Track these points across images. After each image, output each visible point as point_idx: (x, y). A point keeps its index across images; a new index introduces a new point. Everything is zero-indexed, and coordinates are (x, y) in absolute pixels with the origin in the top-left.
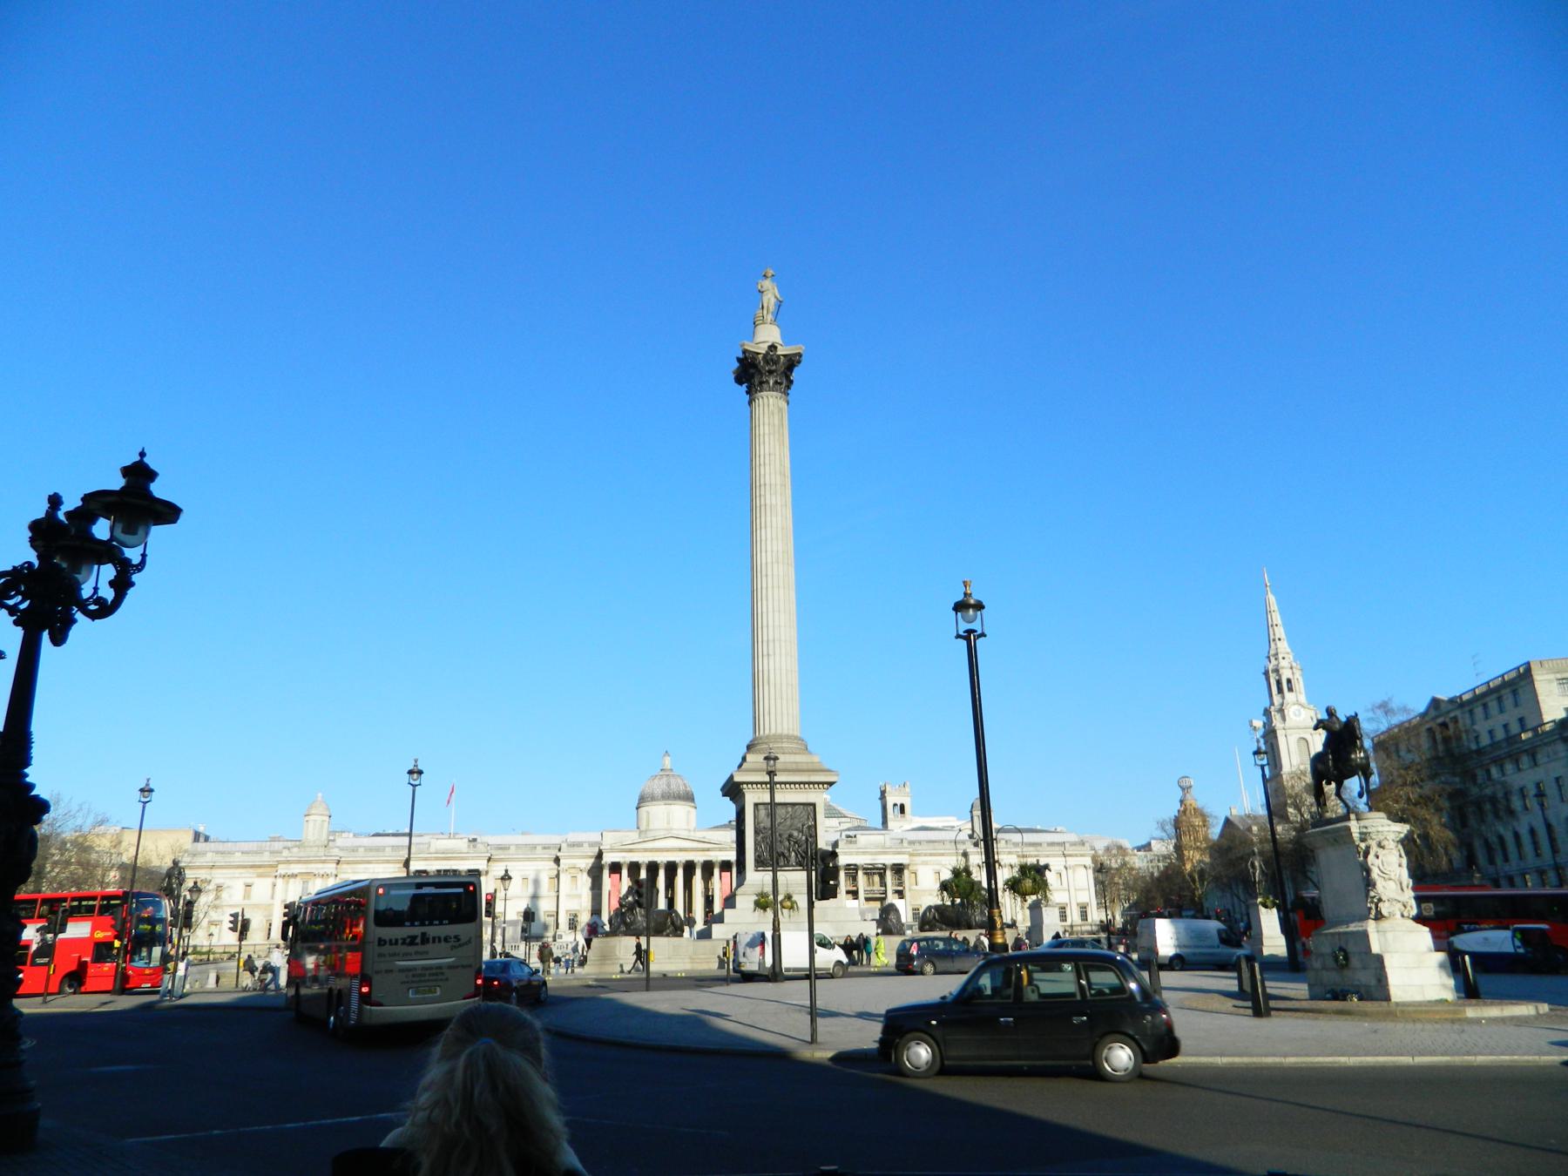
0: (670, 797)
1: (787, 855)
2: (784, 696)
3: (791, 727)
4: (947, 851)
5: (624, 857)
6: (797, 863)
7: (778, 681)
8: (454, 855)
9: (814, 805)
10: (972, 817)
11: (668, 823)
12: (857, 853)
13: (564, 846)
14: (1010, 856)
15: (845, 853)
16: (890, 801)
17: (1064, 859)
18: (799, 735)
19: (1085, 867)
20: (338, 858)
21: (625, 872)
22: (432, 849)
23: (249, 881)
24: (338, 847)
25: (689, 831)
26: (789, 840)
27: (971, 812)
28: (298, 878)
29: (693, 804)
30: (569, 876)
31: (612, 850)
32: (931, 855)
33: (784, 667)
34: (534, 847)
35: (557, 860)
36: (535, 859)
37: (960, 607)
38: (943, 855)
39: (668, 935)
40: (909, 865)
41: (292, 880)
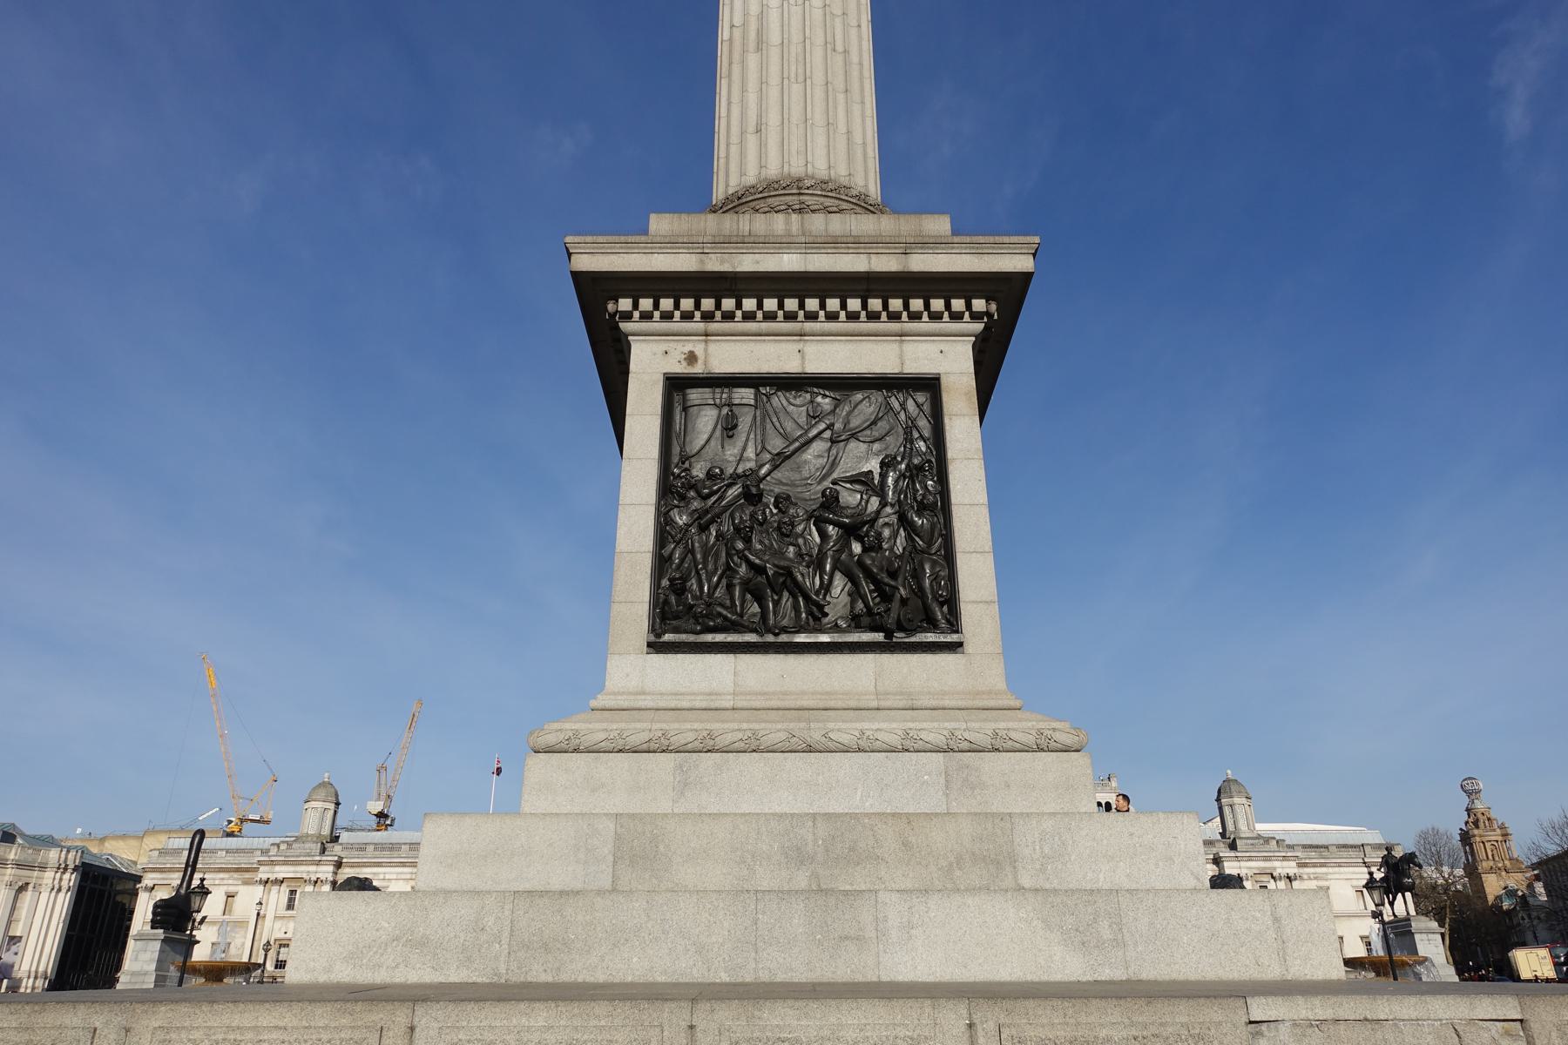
9: (930, 385)
10: (1221, 809)
14: (1285, 864)
17: (1365, 870)
20: (336, 858)
23: (232, 889)
26: (820, 523)
27: (1218, 800)
28: (284, 885)
41: (275, 889)
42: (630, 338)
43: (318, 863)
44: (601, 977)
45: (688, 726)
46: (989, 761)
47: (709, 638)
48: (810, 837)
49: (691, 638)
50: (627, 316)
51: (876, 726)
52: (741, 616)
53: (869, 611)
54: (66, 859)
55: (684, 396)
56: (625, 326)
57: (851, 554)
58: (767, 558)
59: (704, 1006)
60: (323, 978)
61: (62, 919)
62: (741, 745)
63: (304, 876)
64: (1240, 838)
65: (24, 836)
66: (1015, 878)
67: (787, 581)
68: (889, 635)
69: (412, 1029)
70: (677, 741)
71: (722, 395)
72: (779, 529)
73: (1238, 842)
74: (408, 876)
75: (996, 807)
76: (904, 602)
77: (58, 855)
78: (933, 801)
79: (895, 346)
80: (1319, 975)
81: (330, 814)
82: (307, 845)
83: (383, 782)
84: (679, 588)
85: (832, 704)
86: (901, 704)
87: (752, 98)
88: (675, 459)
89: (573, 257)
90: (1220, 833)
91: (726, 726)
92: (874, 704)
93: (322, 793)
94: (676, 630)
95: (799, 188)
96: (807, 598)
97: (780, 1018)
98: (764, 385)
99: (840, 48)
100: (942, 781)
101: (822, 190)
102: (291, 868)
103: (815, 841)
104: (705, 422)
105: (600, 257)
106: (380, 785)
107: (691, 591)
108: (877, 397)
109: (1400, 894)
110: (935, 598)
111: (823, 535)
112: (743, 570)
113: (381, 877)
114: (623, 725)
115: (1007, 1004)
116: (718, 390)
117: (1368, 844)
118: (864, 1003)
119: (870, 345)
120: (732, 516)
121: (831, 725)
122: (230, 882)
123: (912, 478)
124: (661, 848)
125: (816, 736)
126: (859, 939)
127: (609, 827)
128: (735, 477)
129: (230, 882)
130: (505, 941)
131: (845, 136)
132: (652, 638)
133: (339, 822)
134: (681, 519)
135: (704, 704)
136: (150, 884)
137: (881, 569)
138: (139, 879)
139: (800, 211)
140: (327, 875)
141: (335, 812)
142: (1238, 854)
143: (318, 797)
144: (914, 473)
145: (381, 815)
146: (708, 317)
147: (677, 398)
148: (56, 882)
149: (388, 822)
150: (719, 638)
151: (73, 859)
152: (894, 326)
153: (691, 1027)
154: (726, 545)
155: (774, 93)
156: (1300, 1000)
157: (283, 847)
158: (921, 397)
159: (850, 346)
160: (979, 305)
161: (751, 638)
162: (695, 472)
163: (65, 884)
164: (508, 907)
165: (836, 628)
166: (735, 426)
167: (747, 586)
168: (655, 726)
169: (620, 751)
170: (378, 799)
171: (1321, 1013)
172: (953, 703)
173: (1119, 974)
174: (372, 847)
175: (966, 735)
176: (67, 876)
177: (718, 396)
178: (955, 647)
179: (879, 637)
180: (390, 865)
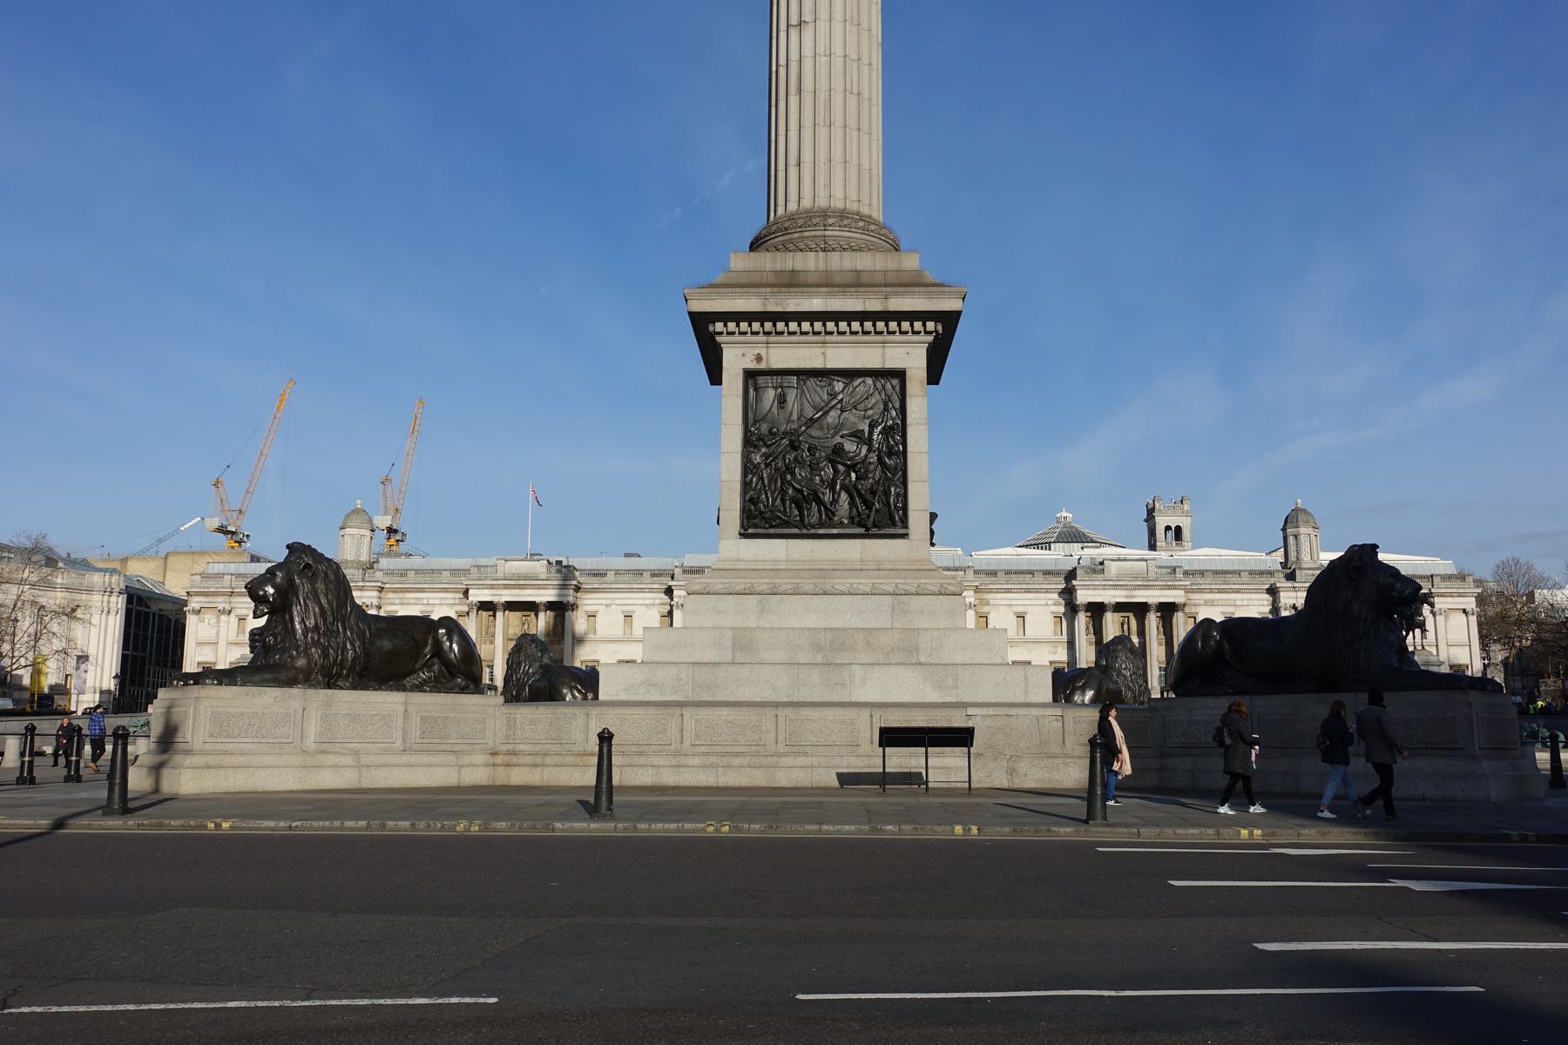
2: (838, 121)
4: (1245, 587)
6: (851, 518)
7: (823, 85)
8: (527, 582)
9: (900, 375)
10: (1285, 539)
12: (1105, 587)
13: (678, 572)
15: (1087, 587)
16: (1161, 522)
18: (877, 214)
19: (1464, 611)
20: (379, 584)
22: (500, 574)
24: (382, 570)
26: (833, 463)
27: (1284, 530)
32: (1220, 591)
33: (838, 51)
34: (639, 573)
35: (669, 592)
36: (641, 590)
38: (1237, 591)
39: (419, 688)
40: (1184, 605)
42: (722, 345)
44: (732, 699)
45: (764, 581)
46: (915, 602)
47: (772, 531)
48: (823, 639)
49: (763, 531)
50: (721, 333)
51: (858, 581)
53: (859, 514)
54: (110, 582)
55: (755, 381)
56: (718, 339)
57: (851, 481)
58: (803, 484)
59: (780, 708)
60: (615, 699)
61: (116, 639)
62: (791, 591)
64: (1301, 569)
66: (918, 658)
68: (867, 530)
69: (682, 715)
70: (759, 589)
71: (777, 380)
72: (810, 466)
73: (1297, 571)
74: (452, 602)
75: (916, 625)
76: (877, 511)
77: (102, 580)
78: (884, 621)
79: (881, 349)
80: (1041, 701)
85: (838, 567)
86: (873, 567)
88: (751, 422)
89: (689, 302)
90: (1281, 563)
91: (782, 581)
92: (859, 567)
93: (357, 520)
94: (756, 526)
95: (825, 226)
96: (826, 507)
97: (806, 712)
98: (802, 375)
99: (855, 91)
100: (890, 609)
101: (840, 226)
103: (826, 640)
104: (770, 395)
105: (705, 302)
107: (762, 502)
108: (869, 381)
109: (1411, 633)
110: (895, 506)
111: (836, 471)
112: (790, 491)
113: (425, 602)
114: (730, 580)
115: (885, 709)
116: (775, 377)
117: (1438, 575)
118: (835, 708)
119: (864, 349)
120: (784, 457)
121: (836, 581)
123: (887, 435)
124: (754, 643)
125: (828, 587)
127: (729, 634)
128: (785, 433)
130: (690, 685)
131: (856, 168)
132: (742, 531)
134: (757, 458)
135: (771, 567)
136: (197, 607)
137: (866, 491)
138: (185, 603)
139: (824, 250)
140: (371, 600)
142: (1295, 585)
143: (354, 524)
144: (887, 431)
145: (391, 531)
148: (105, 604)
150: (779, 531)
151: (117, 582)
152: (879, 338)
153: (776, 715)
154: (781, 476)
156: (985, 708)
158: (895, 382)
159: (852, 350)
160: (930, 325)
161: (796, 531)
162: (763, 430)
163: (113, 605)
164: (690, 670)
165: (841, 525)
166: (785, 401)
167: (793, 500)
168: (747, 581)
169: (730, 594)
170: (386, 513)
171: (992, 713)
172: (901, 567)
173: (954, 700)
174: (413, 573)
175: (904, 587)
176: (113, 599)
177: (775, 381)
178: (904, 536)
179: (862, 531)
180: (433, 590)
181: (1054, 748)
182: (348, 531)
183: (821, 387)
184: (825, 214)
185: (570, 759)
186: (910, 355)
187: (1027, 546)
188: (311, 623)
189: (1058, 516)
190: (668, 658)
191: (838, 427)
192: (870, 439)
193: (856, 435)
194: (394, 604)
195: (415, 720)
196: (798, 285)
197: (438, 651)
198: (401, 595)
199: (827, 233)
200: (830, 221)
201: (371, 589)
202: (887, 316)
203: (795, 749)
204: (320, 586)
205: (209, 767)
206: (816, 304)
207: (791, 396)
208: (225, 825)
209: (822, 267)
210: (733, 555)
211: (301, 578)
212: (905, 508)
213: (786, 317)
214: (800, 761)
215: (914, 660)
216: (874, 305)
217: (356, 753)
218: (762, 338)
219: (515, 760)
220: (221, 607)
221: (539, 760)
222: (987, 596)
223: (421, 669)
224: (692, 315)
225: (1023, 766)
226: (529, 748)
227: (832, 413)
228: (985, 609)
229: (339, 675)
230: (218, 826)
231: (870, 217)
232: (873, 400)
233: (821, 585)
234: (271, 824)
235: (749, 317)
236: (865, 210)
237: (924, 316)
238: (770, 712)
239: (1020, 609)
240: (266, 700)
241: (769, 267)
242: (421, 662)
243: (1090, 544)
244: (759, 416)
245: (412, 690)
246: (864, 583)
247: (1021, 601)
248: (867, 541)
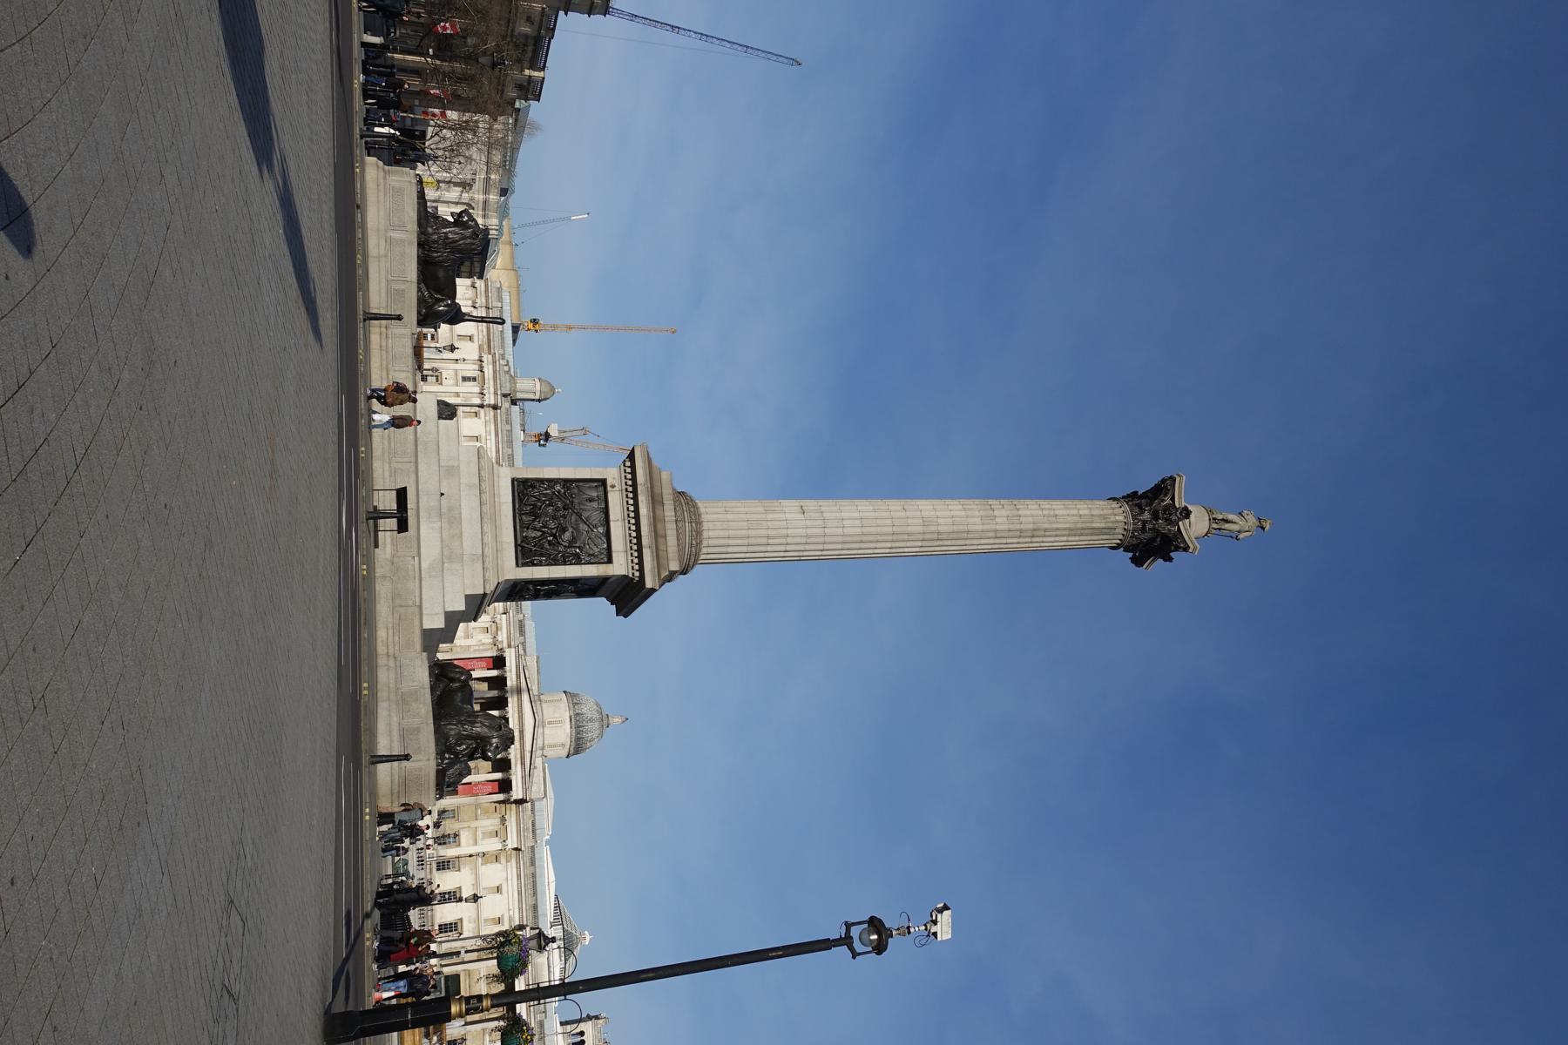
0: (578, 723)
1: (538, 525)
3: (711, 542)
5: (511, 671)
6: (526, 537)
9: (610, 561)
11: (550, 723)
20: (499, 405)
21: (494, 673)
23: (476, 338)
25: (543, 749)
28: (479, 372)
29: (572, 751)
30: (487, 625)
31: (518, 657)
37: (875, 924)
39: (419, 290)
41: (477, 367)
43: (496, 393)
49: (516, 489)
52: (525, 504)
63: (486, 386)
65: (506, 200)
67: (537, 517)
70: (483, 484)
81: (532, 397)
82: (508, 384)
83: (574, 433)
84: (533, 487)
87: (742, 509)
93: (547, 389)
94: (518, 486)
102: (491, 376)
106: (572, 431)
108: (605, 546)
113: (488, 438)
122: (480, 337)
126: (429, 518)
127: (456, 464)
128: (572, 502)
129: (480, 337)
133: (526, 403)
134: (558, 487)
136: (477, 285)
138: (481, 277)
139: (676, 521)
141: (533, 400)
145: (547, 436)
146: (626, 490)
147: (600, 484)
149: (542, 442)
155: (743, 516)
157: (506, 368)
158: (606, 560)
160: (637, 574)
161: (517, 506)
165: (522, 532)
166: (590, 501)
167: (535, 506)
170: (560, 432)
174: (509, 428)
178: (517, 565)
179: (519, 542)
180: (497, 443)
181: (398, 602)
182: (538, 384)
183: (600, 521)
184: (699, 523)
185: (385, 363)
186: (620, 566)
187: (558, 907)
188: (450, 236)
189: (586, 932)
190: (441, 432)
191: (577, 529)
192: (571, 547)
193: (573, 540)
194: (485, 416)
195: (403, 287)
196: (653, 503)
197: (438, 301)
198: (492, 421)
199: (687, 524)
200: (694, 525)
201: (496, 399)
202: (640, 550)
203: (393, 471)
204: (468, 241)
205: (378, 186)
206: (643, 511)
207: (595, 505)
208: (358, 170)
209: (666, 519)
210: (502, 474)
211: (472, 232)
212: (534, 565)
213: (635, 498)
214: (387, 474)
215: (445, 560)
216: (645, 541)
217: (386, 256)
218: (624, 487)
219: (384, 336)
220: (478, 301)
221: (384, 348)
222: (514, 860)
223: (430, 293)
224: (633, 450)
225: (387, 583)
226: (390, 345)
227: (585, 526)
228: (503, 860)
229: (424, 249)
230: (357, 167)
231: (700, 550)
232: (595, 548)
233: (486, 515)
234: (359, 187)
235: (634, 479)
236: (704, 550)
237: (641, 570)
238: (413, 460)
239: (504, 889)
240: (411, 214)
241: (664, 491)
242: (433, 292)
243: (563, 958)
244: (581, 488)
245: (418, 287)
246: (489, 539)
247: (511, 888)
248: (513, 545)
